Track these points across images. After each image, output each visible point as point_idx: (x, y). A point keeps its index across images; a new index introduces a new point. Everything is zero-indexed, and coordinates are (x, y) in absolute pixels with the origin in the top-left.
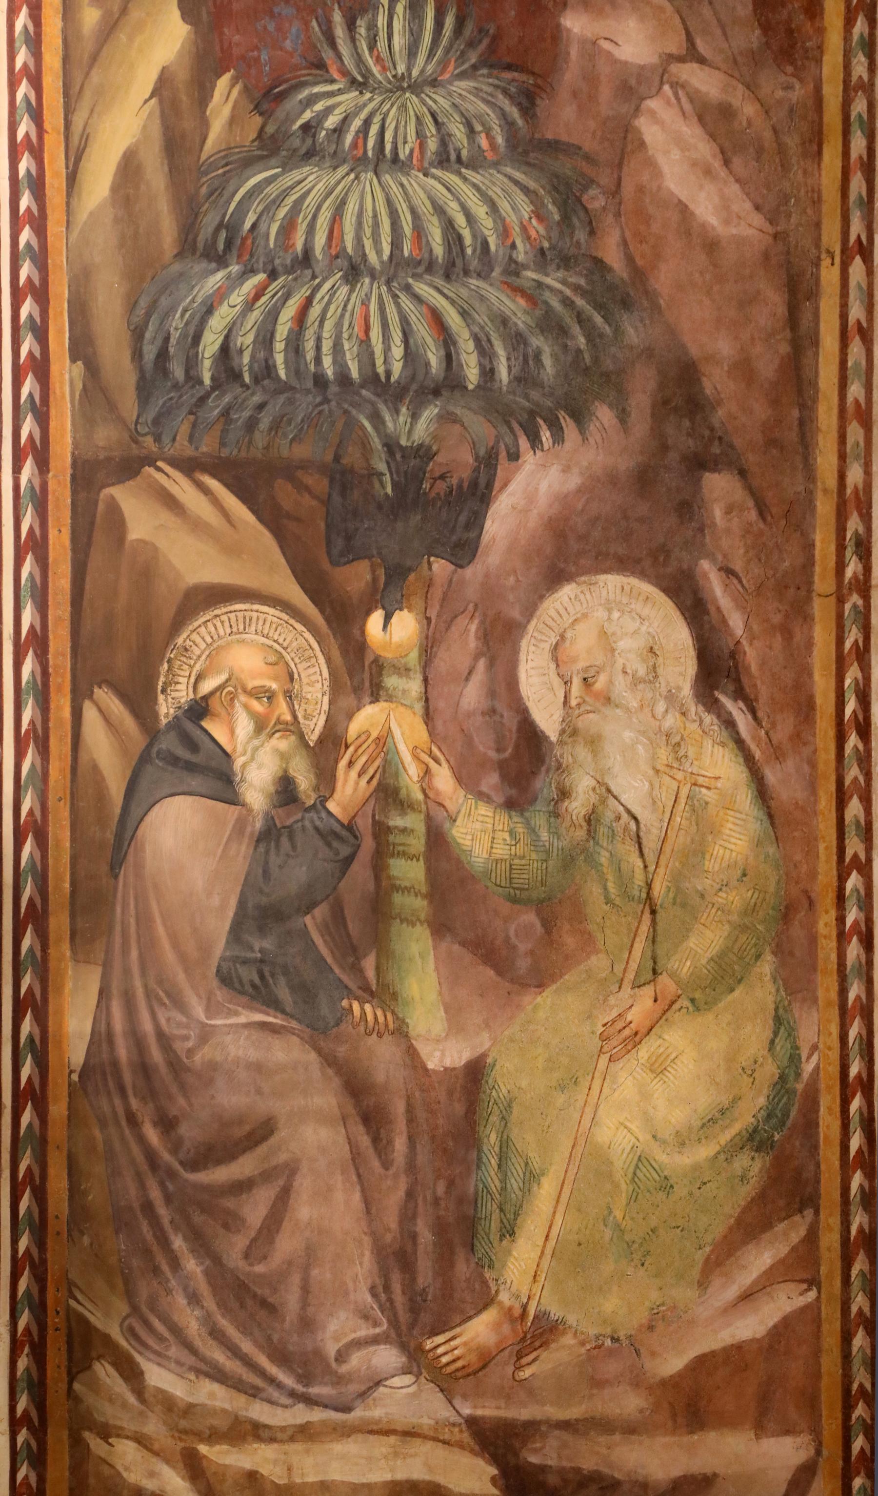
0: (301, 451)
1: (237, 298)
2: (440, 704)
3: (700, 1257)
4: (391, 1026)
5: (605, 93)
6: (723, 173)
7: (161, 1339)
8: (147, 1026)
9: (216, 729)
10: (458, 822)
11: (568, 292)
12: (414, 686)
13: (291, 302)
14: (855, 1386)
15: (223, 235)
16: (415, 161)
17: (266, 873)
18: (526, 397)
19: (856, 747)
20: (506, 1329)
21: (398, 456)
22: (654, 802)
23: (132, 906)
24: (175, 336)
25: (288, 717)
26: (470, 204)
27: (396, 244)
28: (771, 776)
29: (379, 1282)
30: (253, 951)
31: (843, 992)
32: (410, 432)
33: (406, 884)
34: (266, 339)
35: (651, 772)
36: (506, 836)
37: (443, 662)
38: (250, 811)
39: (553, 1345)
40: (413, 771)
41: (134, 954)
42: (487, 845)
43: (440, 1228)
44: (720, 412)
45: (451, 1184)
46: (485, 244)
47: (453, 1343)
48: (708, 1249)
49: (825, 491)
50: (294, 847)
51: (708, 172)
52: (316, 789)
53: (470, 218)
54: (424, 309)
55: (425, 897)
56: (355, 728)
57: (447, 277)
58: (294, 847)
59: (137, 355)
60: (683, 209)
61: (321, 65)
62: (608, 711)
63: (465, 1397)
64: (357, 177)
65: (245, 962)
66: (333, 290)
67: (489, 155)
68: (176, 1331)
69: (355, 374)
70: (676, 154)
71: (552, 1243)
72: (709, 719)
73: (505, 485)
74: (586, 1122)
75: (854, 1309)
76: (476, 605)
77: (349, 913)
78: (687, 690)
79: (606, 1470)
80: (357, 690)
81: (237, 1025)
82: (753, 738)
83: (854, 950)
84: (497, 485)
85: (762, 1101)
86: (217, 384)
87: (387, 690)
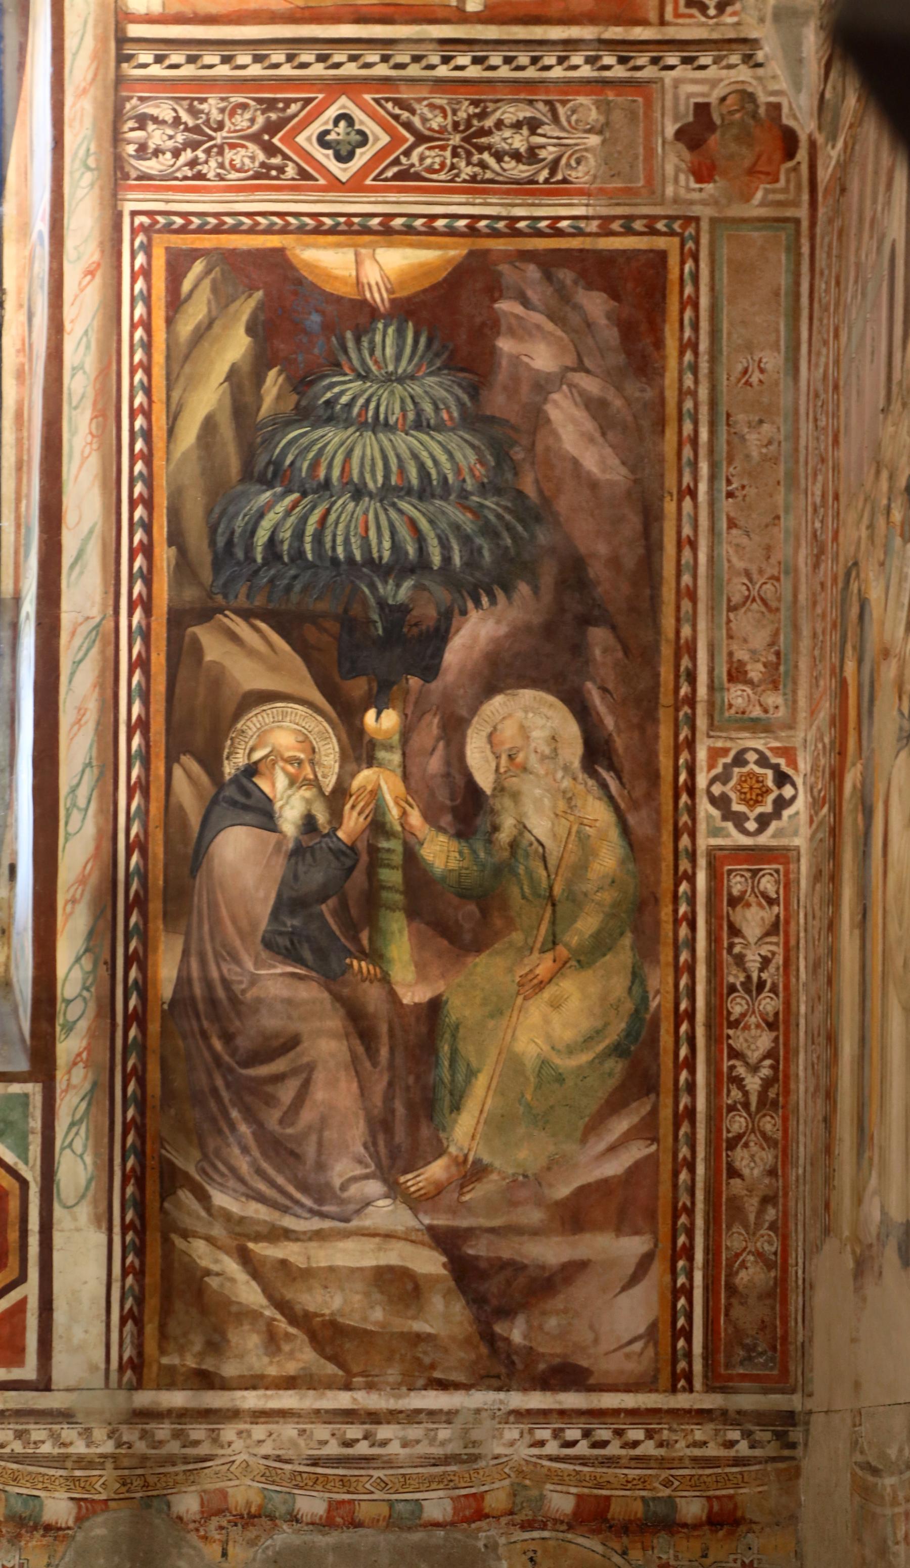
0: (321, 606)
1: (280, 508)
2: (413, 769)
3: (581, 1124)
4: (379, 976)
5: (525, 389)
6: (600, 440)
7: (223, 1175)
8: (215, 974)
10: (425, 845)
11: (500, 510)
13: (316, 511)
14: (680, 1204)
15: (271, 468)
16: (399, 426)
17: (296, 877)
18: (472, 575)
19: (686, 803)
20: (454, 1169)
21: (387, 611)
22: (555, 835)
23: (205, 897)
24: (238, 531)
25: (311, 776)
26: (435, 453)
27: (387, 477)
28: (632, 820)
29: (369, 1139)
30: (285, 925)
31: (676, 957)
32: (395, 596)
33: (390, 884)
34: (299, 534)
35: (552, 816)
36: (457, 855)
38: (285, 836)
39: (485, 1180)
40: (394, 812)
41: (206, 928)
42: (444, 860)
43: (410, 1106)
44: (600, 589)
45: (418, 1078)
46: (445, 479)
47: (418, 1179)
48: (587, 1119)
49: (667, 641)
50: (314, 860)
51: (592, 440)
52: (330, 822)
53: (436, 462)
54: (405, 519)
55: (401, 893)
56: (356, 783)
57: (421, 498)
58: (314, 860)
59: (212, 543)
60: (576, 462)
61: (338, 365)
62: (524, 776)
63: (426, 1212)
64: (361, 435)
65: (281, 934)
66: (344, 505)
67: (449, 423)
68: (233, 1170)
69: (358, 557)
70: (570, 428)
71: (485, 1115)
72: (591, 782)
73: (458, 630)
74: (508, 1038)
75: (681, 1156)
76: (438, 709)
77: (351, 903)
78: (576, 764)
79: (518, 1258)
80: (358, 760)
81: (275, 974)
82: (621, 795)
83: (684, 931)
84: (453, 630)
85: (623, 1025)
86: (266, 562)
87: (377, 759)
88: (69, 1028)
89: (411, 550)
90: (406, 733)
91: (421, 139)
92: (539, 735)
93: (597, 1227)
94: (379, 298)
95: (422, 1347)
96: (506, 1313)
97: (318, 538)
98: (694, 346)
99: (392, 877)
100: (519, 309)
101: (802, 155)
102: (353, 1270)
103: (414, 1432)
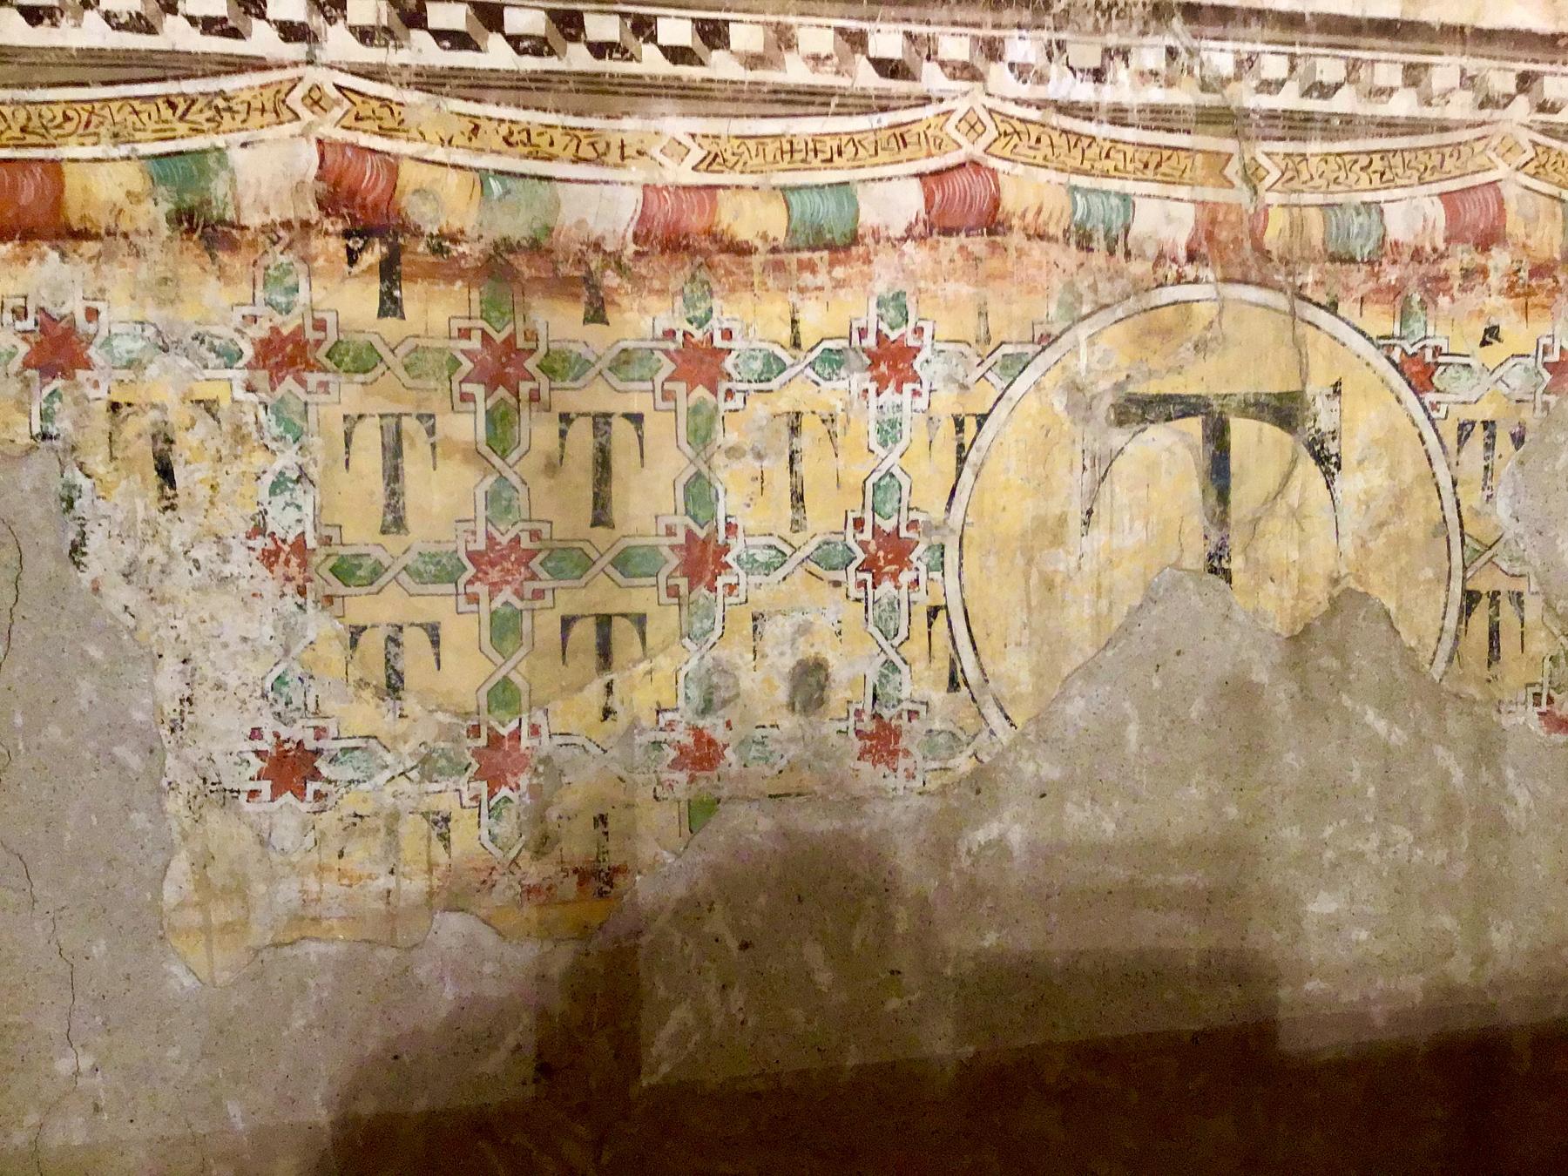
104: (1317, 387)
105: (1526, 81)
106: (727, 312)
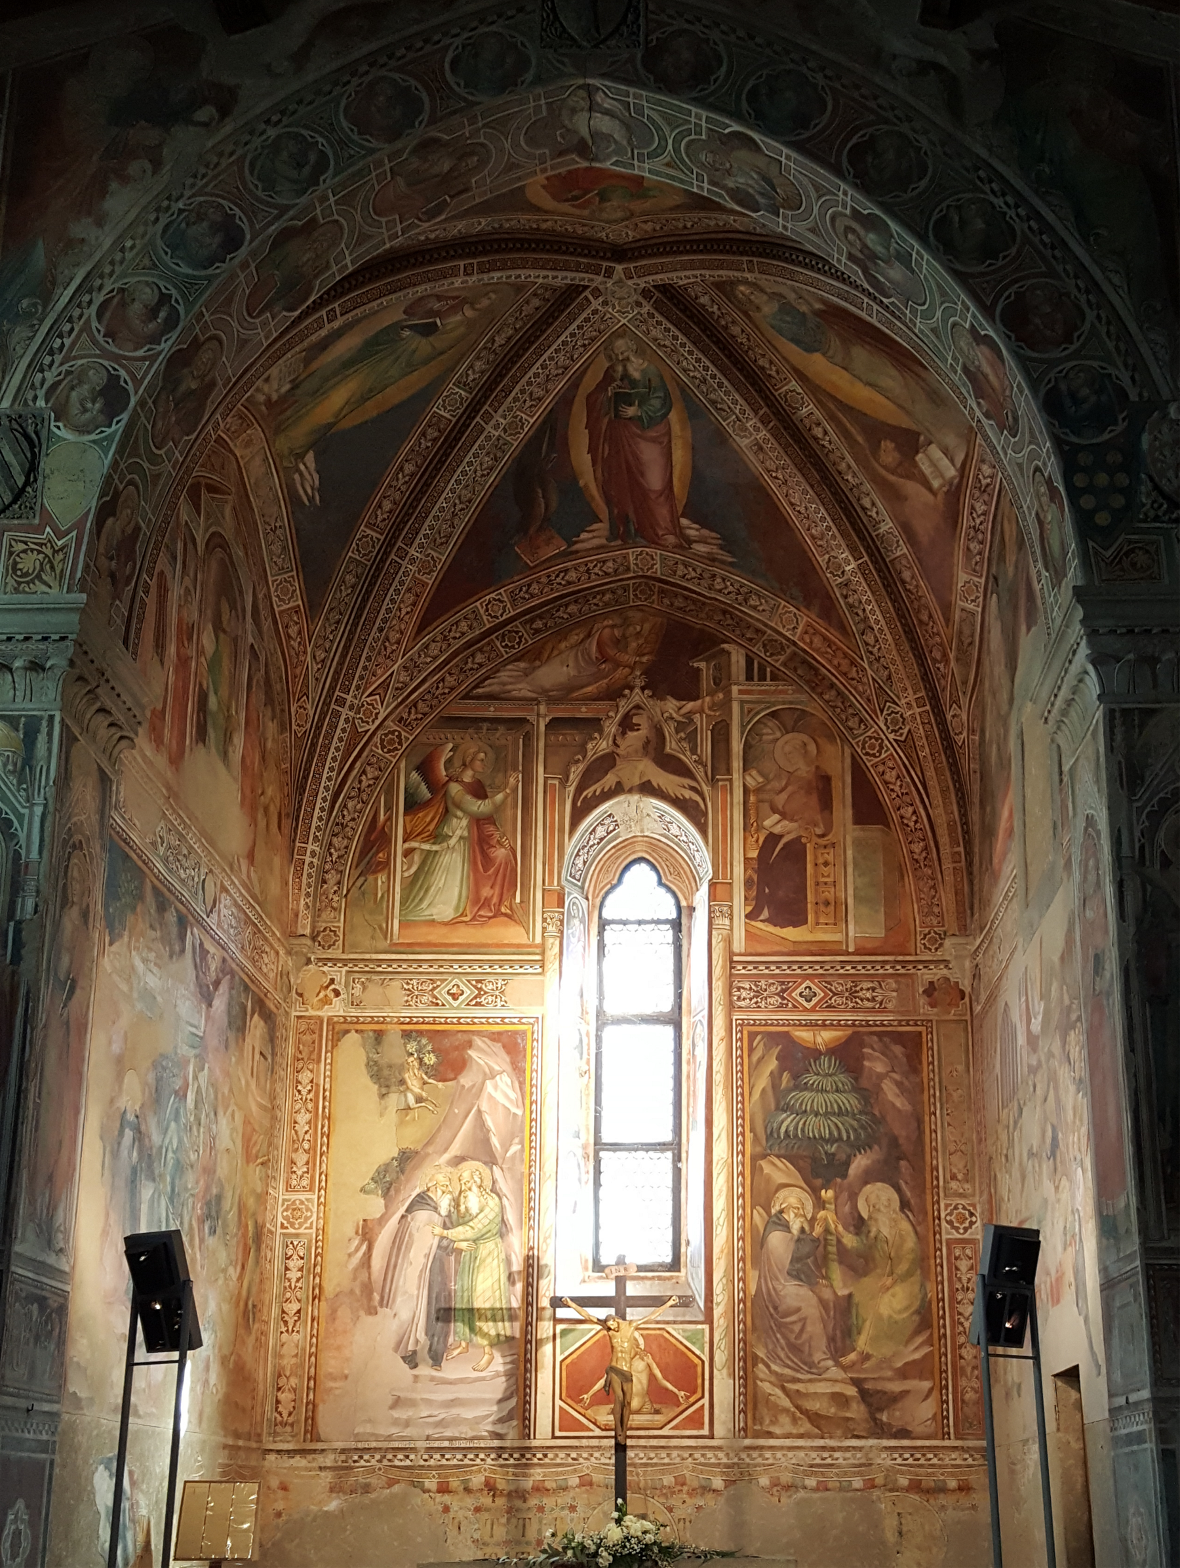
1: (789, 1119)
9: (786, 1216)
12: (833, 1207)
28: (918, 1229)
34: (796, 1128)
37: (839, 1201)
40: (833, 1226)
43: (842, 1332)
60: (893, 1105)
83: (939, 1268)
88: (718, 1304)
89: (836, 1134)
90: (836, 1198)
91: (835, 994)
92: (884, 1199)
93: (914, 1378)
94: (822, 1048)
95: (850, 1422)
96: (881, 1410)
97: (803, 1130)
98: (933, 1063)
99: (832, 1249)
100: (870, 1051)
101: (967, 999)
102: (824, 1394)
103: (848, 1455)
104: (650, 1513)
105: (691, 1455)
106: (545, 1501)
